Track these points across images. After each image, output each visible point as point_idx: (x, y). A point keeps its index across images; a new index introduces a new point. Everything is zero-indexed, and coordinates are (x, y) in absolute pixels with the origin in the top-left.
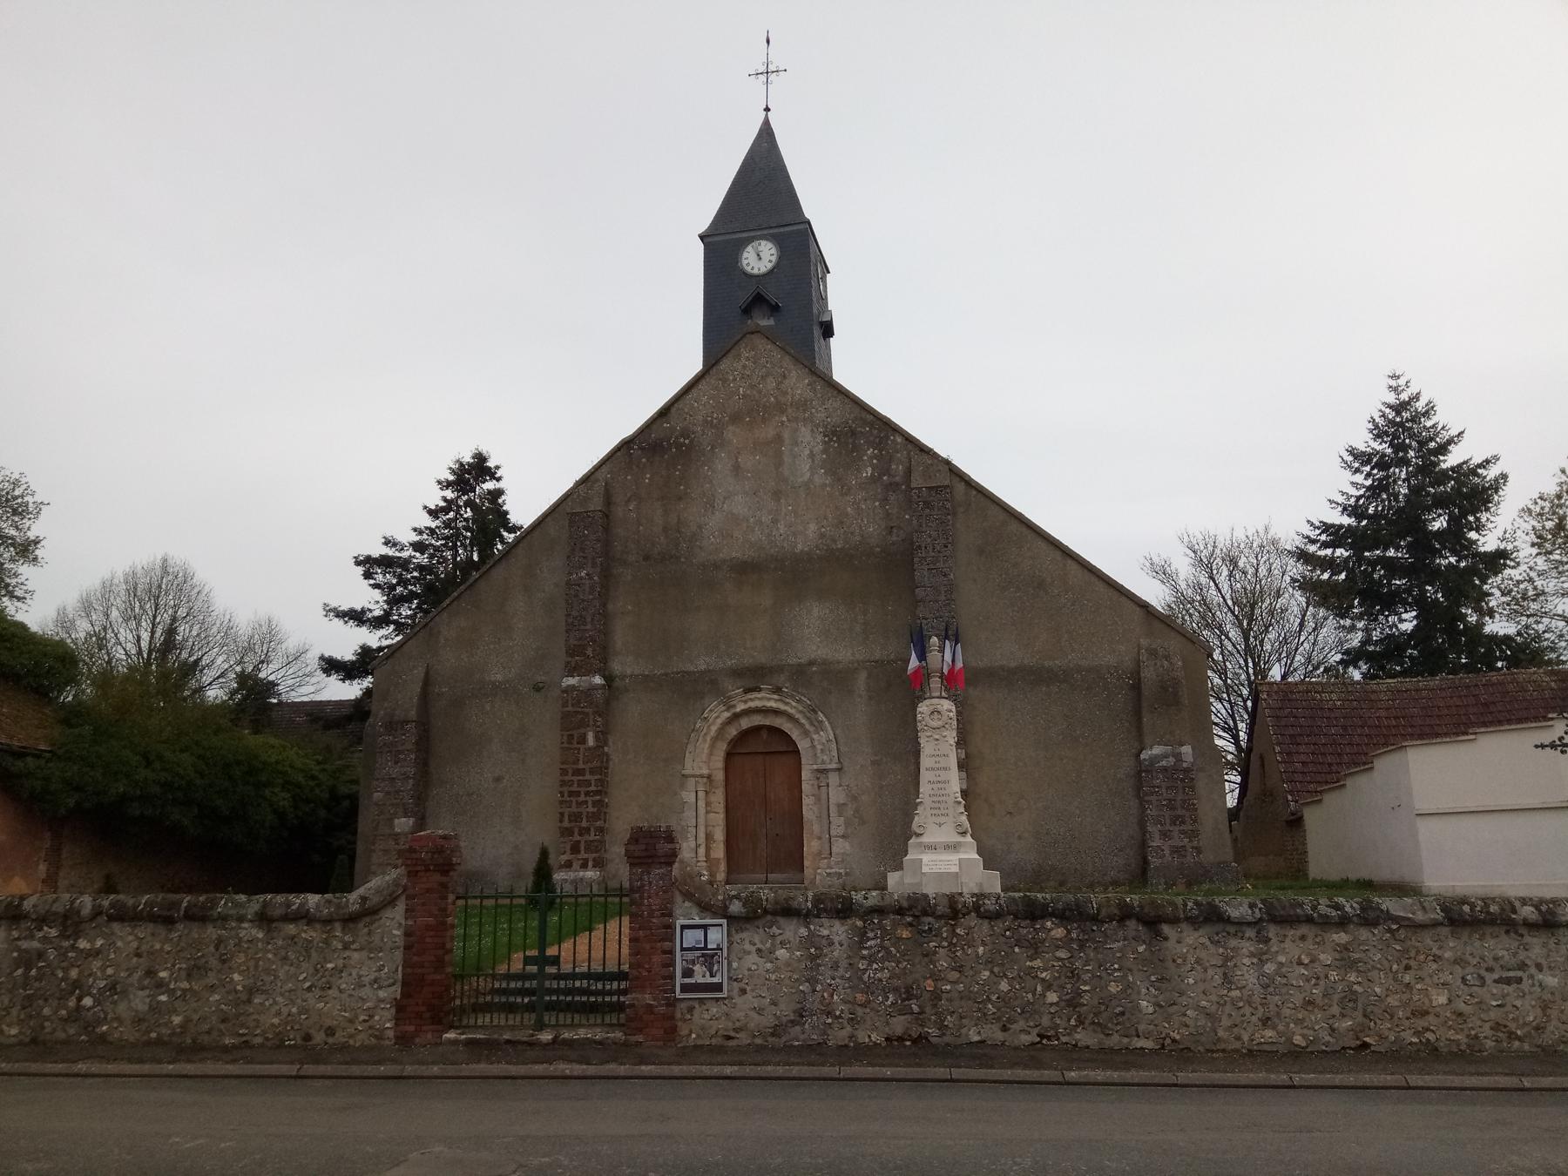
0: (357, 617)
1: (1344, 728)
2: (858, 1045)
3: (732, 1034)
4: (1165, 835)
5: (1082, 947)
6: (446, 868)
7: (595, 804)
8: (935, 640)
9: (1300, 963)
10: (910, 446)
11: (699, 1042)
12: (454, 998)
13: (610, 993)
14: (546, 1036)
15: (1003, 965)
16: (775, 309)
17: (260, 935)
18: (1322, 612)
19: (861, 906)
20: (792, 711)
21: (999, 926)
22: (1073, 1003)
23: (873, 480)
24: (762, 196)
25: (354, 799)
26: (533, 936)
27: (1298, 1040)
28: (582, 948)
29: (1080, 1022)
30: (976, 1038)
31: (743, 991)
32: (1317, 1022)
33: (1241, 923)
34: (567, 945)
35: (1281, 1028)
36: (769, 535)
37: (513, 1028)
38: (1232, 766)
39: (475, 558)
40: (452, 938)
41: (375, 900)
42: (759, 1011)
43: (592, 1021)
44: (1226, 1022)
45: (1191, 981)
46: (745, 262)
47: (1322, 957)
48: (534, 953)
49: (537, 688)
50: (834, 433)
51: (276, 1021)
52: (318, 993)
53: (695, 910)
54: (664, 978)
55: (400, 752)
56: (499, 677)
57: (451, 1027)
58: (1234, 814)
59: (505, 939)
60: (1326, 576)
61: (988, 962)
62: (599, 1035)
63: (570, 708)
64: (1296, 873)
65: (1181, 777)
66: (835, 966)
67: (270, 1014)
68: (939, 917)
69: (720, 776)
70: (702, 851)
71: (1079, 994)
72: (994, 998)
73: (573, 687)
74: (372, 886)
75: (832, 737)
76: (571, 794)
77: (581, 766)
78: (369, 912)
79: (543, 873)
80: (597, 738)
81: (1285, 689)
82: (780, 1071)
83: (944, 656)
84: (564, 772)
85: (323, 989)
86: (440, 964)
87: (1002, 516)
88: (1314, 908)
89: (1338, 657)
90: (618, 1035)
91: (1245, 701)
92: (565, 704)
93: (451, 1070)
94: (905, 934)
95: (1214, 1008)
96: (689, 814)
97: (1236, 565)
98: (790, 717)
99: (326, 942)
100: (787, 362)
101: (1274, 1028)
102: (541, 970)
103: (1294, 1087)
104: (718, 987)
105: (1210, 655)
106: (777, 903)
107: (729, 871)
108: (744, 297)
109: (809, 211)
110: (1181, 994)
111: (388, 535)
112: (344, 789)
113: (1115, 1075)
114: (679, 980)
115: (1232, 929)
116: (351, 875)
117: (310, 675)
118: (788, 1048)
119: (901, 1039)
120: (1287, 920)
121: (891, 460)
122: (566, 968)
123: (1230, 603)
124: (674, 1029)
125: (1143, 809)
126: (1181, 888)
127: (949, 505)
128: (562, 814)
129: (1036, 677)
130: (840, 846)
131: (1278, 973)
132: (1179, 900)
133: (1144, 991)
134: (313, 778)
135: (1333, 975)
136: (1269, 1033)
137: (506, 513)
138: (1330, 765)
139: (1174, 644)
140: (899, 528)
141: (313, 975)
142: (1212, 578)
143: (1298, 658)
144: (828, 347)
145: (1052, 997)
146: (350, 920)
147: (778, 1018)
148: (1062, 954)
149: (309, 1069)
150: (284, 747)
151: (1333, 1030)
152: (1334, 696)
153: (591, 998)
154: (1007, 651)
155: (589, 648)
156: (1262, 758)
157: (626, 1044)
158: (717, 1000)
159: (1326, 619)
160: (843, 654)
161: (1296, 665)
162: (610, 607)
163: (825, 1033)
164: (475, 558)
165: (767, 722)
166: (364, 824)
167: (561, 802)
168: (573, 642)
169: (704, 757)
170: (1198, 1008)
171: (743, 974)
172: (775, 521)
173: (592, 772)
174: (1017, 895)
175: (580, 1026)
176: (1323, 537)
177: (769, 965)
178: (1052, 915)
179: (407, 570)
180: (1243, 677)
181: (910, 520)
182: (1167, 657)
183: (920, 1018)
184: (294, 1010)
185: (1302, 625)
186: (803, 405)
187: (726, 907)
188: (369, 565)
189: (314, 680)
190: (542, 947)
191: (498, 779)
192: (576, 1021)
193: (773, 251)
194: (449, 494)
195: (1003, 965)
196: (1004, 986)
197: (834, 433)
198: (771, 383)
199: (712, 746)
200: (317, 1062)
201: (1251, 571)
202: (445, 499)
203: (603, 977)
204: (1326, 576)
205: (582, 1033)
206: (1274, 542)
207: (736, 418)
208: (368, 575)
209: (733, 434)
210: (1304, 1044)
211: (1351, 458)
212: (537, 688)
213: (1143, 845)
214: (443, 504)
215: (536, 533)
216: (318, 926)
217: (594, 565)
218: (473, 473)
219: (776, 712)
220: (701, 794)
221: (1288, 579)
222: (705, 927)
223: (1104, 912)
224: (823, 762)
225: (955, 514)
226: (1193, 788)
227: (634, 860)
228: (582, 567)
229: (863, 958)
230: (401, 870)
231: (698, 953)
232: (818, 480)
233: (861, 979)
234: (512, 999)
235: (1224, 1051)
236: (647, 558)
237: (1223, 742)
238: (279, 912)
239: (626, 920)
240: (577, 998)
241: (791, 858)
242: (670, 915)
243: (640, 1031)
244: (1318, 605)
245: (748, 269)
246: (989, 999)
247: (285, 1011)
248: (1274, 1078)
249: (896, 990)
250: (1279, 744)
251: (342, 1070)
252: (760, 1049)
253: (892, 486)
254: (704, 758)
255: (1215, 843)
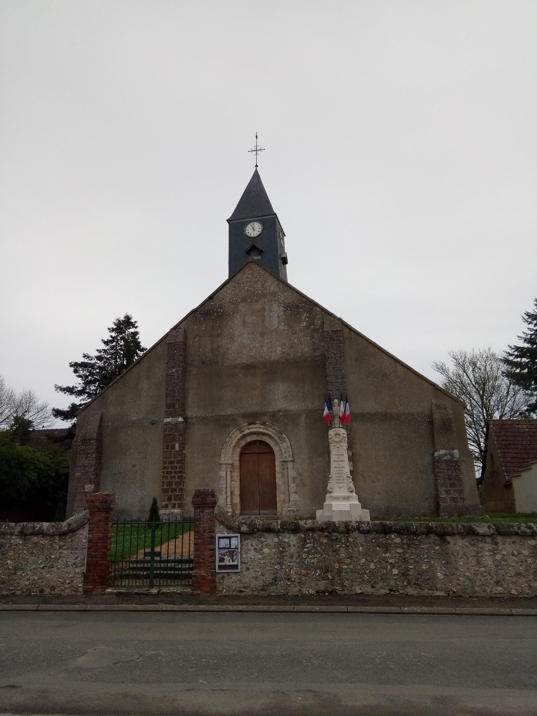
0: (70, 390)
1: (530, 441)
2: (303, 595)
3: (243, 590)
4: (447, 492)
5: (409, 547)
6: (108, 510)
7: (179, 477)
8: (336, 401)
9: (513, 554)
10: (323, 312)
11: (228, 594)
12: (112, 572)
13: (185, 569)
14: (154, 591)
15: (371, 556)
16: (261, 252)
17: (21, 542)
18: (517, 387)
19: (304, 527)
20: (270, 433)
21: (369, 537)
22: (405, 574)
23: (307, 327)
24: (254, 203)
25: (67, 475)
26: (149, 541)
27: (514, 592)
28: (172, 547)
29: (409, 583)
30: (359, 591)
31: (248, 569)
32: (523, 583)
33: (484, 536)
34: (165, 546)
35: (505, 586)
36: (259, 352)
37: (138, 587)
38: (477, 459)
39: (125, 363)
40: (110, 544)
41: (75, 525)
42: (256, 578)
43: (176, 583)
44: (478, 583)
45: (461, 563)
46: (247, 232)
47: (524, 552)
48: (148, 550)
49: (152, 423)
50: (288, 307)
51: (27, 583)
52: (47, 569)
53: (225, 530)
54: (211, 562)
55: (88, 454)
56: (135, 418)
57: (109, 586)
58: (479, 481)
59: (136, 543)
60: (518, 371)
61: (364, 555)
62: (179, 590)
63: (167, 433)
64: (509, 509)
65: (454, 465)
66: (292, 556)
67: (26, 579)
68: (340, 533)
69: (237, 464)
70: (229, 500)
71: (408, 570)
72: (367, 572)
73: (169, 423)
74: (72, 519)
75: (289, 445)
76: (168, 473)
77: (172, 459)
78: (72, 531)
79: (154, 510)
80: (180, 447)
81: (501, 423)
82: (266, 608)
83: (340, 408)
84: (164, 462)
85: (49, 568)
86: (104, 556)
87: (366, 344)
88: (519, 528)
89: (526, 408)
90: (189, 590)
91: (483, 428)
92: (165, 431)
93: (109, 607)
94: (325, 541)
95: (472, 576)
96: (223, 482)
97: (476, 366)
98: (269, 436)
99: (51, 545)
100: (267, 275)
101: (502, 586)
102: (152, 558)
103: (512, 615)
104: (236, 567)
105: (465, 407)
106: (263, 526)
107: (242, 509)
108: (247, 247)
109: (275, 211)
110: (457, 569)
111: (85, 353)
112: (62, 471)
113: (426, 609)
114: (217, 563)
115: (480, 539)
116: (65, 512)
117: (48, 417)
118: (269, 596)
119: (323, 592)
120: (507, 534)
121: (314, 319)
122: (164, 557)
123: (474, 383)
124: (215, 587)
125: (436, 480)
126: (455, 517)
127: (341, 339)
128: (163, 482)
129: (384, 418)
130: (294, 497)
131: (502, 559)
132: (454, 524)
133: (439, 568)
134: (48, 466)
135: (530, 560)
136: (499, 588)
137: (139, 342)
138: (524, 458)
139: (448, 403)
140: (319, 349)
141: (45, 561)
142: (464, 371)
143: (507, 408)
144: (285, 269)
145: (395, 571)
146: (63, 535)
147: (265, 582)
148: (400, 550)
149: (43, 607)
150: (35, 452)
151: (530, 587)
152: (524, 427)
153: (175, 572)
154: (370, 406)
155: (176, 404)
156: (492, 455)
157: (192, 595)
158: (236, 573)
159: (519, 390)
160: (294, 407)
161: (506, 411)
162: (186, 385)
163: (287, 589)
164: (125, 363)
165: (259, 439)
166: (71, 488)
167: (163, 477)
168: (169, 401)
169: (230, 455)
170: (464, 576)
171: (247, 560)
172: (262, 346)
173: (178, 462)
174: (377, 522)
175: (170, 586)
176: (516, 353)
177: (260, 556)
178: (394, 532)
179: (94, 369)
180: (481, 417)
181: (324, 346)
182: (445, 409)
183: (332, 582)
184: (36, 578)
185: (508, 393)
186: (274, 294)
187: (239, 528)
188: (76, 366)
189: (50, 420)
190: (153, 547)
191: (134, 466)
192: (169, 584)
193: (260, 227)
194: (114, 334)
195: (371, 556)
196: (372, 566)
197: (288, 307)
198: (259, 285)
199: (234, 450)
200: (46, 603)
201: (483, 368)
202: (111, 336)
203: (181, 561)
204: (518, 371)
205: (172, 589)
206: (493, 355)
207: (244, 300)
208: (75, 371)
209: (243, 307)
210: (516, 594)
211: (527, 317)
212: (152, 423)
213: (437, 497)
214: (111, 339)
215: (153, 352)
216: (48, 538)
217: (179, 366)
218: (125, 325)
219: (263, 434)
220: (228, 473)
221: (500, 372)
222: (230, 538)
223: (419, 531)
224: (285, 458)
225: (344, 343)
226: (460, 470)
227: (196, 506)
228: (173, 367)
229: (305, 552)
230: (87, 511)
231: (226, 550)
232: (281, 327)
233: (304, 563)
234: (138, 572)
235: (478, 597)
236: (203, 363)
237: (473, 447)
238: (29, 531)
239: (192, 533)
240: (169, 572)
241: (270, 502)
242: (213, 532)
243: (199, 588)
244: (515, 384)
245: (249, 235)
246: (365, 573)
247: (32, 578)
248: (503, 611)
249: (320, 568)
250: (500, 449)
251: (57, 607)
252: (256, 597)
253: (315, 330)
254: (230, 456)
255: (471, 496)
